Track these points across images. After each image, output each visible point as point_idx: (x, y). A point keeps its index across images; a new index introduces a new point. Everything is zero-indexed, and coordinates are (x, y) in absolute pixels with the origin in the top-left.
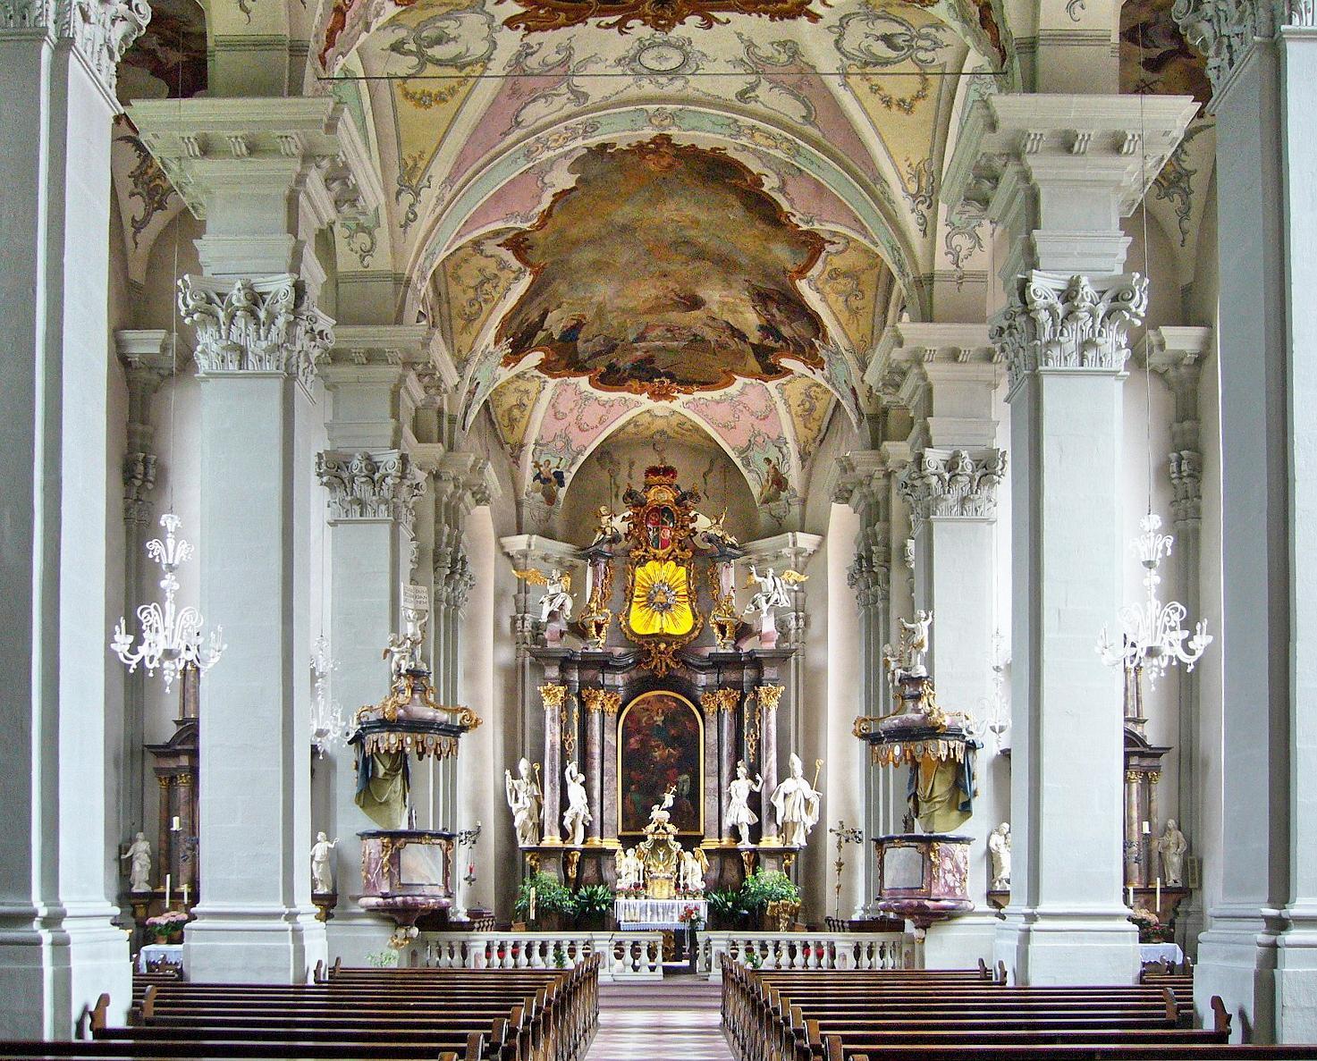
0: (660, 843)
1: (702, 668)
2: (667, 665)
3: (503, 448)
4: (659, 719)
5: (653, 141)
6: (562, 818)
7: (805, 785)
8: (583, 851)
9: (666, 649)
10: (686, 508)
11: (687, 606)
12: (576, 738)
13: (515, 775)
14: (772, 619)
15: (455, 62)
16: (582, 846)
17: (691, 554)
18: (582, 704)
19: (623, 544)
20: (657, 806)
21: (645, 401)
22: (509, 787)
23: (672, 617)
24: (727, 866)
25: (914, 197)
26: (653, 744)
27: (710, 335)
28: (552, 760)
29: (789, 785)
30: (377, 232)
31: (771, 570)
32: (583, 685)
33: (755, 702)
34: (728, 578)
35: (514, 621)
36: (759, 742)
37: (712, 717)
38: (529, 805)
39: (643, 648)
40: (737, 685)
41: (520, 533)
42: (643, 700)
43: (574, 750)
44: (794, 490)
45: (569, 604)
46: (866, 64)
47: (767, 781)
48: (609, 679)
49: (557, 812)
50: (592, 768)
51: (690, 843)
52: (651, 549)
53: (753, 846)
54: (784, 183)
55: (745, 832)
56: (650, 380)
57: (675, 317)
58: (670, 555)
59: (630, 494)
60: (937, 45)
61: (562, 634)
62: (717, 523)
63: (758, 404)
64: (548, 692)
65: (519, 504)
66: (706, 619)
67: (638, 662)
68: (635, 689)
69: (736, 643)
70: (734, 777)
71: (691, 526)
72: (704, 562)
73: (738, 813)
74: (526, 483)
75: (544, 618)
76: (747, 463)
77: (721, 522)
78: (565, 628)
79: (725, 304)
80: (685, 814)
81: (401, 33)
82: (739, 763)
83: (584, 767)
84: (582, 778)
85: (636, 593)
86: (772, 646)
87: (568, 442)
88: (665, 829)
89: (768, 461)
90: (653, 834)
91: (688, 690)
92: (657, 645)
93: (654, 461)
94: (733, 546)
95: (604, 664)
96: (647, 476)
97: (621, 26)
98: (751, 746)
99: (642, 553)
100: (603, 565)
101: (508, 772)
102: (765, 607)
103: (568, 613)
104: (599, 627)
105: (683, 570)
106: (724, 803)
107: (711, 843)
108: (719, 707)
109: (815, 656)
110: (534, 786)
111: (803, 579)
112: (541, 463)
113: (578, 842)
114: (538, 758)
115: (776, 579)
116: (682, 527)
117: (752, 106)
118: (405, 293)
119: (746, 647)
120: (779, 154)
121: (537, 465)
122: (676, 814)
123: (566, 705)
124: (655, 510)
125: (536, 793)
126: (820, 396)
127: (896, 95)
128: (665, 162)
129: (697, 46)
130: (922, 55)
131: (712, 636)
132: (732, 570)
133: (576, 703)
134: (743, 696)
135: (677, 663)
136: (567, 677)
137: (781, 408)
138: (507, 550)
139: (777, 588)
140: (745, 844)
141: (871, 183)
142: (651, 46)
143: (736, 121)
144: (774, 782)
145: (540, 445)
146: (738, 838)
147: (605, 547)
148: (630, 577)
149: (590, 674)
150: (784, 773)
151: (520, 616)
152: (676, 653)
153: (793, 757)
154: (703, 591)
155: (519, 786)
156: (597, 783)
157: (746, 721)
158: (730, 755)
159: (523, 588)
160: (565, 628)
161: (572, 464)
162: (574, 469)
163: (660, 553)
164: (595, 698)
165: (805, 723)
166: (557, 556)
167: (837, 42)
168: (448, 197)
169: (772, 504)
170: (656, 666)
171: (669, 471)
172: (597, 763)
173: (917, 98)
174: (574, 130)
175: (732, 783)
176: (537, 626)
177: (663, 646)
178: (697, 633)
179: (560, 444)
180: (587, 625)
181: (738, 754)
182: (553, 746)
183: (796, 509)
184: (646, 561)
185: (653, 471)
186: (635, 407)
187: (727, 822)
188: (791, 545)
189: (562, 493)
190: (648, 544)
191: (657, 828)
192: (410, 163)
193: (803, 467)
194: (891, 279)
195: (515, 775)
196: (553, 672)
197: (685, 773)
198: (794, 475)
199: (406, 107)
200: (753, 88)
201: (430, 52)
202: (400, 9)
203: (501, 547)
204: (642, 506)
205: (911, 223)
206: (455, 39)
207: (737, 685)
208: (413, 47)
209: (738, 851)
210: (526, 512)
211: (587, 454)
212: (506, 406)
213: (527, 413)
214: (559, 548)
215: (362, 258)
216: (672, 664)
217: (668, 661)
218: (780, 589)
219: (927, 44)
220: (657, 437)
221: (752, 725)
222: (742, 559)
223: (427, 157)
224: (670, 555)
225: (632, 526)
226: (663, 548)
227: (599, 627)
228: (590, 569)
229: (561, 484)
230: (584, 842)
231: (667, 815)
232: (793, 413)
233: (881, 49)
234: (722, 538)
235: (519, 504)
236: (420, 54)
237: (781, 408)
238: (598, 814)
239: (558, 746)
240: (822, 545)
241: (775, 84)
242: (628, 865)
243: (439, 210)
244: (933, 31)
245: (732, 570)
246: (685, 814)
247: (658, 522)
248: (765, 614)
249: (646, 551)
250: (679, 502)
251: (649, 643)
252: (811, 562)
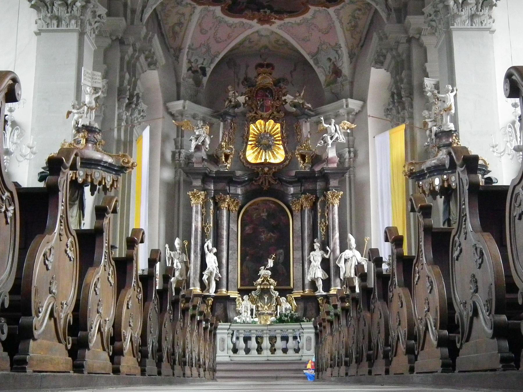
0: (265, 291)
1: (291, 183)
2: (269, 182)
3: (169, 51)
4: (264, 215)
6: (202, 275)
7: (358, 254)
8: (215, 298)
9: (268, 171)
10: (280, 88)
11: (281, 147)
12: (211, 225)
13: (172, 248)
14: (334, 150)
16: (214, 294)
17: (283, 115)
18: (216, 204)
19: (241, 109)
20: (263, 267)
21: (255, 25)
22: (168, 255)
23: (273, 153)
24: (309, 309)
26: (261, 230)
28: (196, 238)
29: (347, 253)
31: (333, 121)
32: (216, 191)
33: (326, 204)
34: (306, 128)
35: (174, 154)
36: (327, 227)
37: (297, 214)
38: (180, 267)
39: (255, 171)
40: (313, 192)
41: (178, 99)
42: (254, 203)
43: (211, 232)
44: (345, 76)
45: (208, 141)
47: (333, 251)
48: (232, 190)
49: (198, 272)
50: (222, 244)
51: (283, 293)
52: (260, 112)
53: (325, 293)
55: (320, 284)
56: (258, 10)
58: (270, 115)
59: (246, 79)
61: (203, 160)
62: (300, 95)
63: (321, 22)
64: (194, 196)
65: (178, 85)
66: (293, 154)
67: (250, 180)
68: (248, 196)
69: (312, 166)
70: (312, 249)
71: (283, 98)
72: (291, 121)
73: (316, 272)
74: (183, 75)
75: (192, 150)
76: (317, 62)
77: (302, 94)
78: (205, 157)
80: (281, 273)
82: (315, 240)
83: (217, 243)
84: (215, 250)
85: (250, 139)
86: (335, 165)
87: (208, 50)
88: (268, 281)
89: (330, 59)
90: (260, 284)
91: (282, 196)
92: (263, 169)
93: (259, 61)
94: (310, 109)
95: (229, 179)
96: (256, 68)
98: (323, 230)
99: (254, 115)
100: (229, 121)
101: (167, 246)
102: (330, 142)
103: (207, 146)
104: (227, 157)
105: (278, 125)
106: (306, 266)
107: (297, 293)
108: (302, 206)
109: (360, 174)
110: (184, 255)
111: (353, 126)
112: (192, 60)
113: (212, 291)
114: (187, 236)
115: (337, 126)
116: (278, 99)
119: (317, 169)
121: (190, 62)
122: (275, 272)
123: (205, 205)
124: (261, 88)
125: (185, 260)
126: (361, 17)
131: (297, 163)
132: (308, 124)
133: (212, 203)
134: (317, 199)
135: (275, 180)
136: (207, 187)
137: (337, 24)
138: (170, 111)
139: (336, 131)
140: (321, 292)
144: (338, 251)
145: (193, 49)
146: (315, 289)
147: (231, 111)
148: (246, 129)
149: (221, 186)
150: (344, 246)
151: (177, 151)
152: (274, 174)
153: (350, 236)
154: (290, 138)
155: (174, 255)
156: (225, 254)
157: (319, 214)
158: (309, 236)
159: (180, 133)
160: (205, 157)
161: (212, 62)
162: (213, 66)
163: (265, 114)
164: (224, 200)
165: (357, 216)
166: (201, 115)
169: (333, 86)
170: (262, 183)
171: (268, 65)
172: (225, 241)
175: (311, 253)
176: (189, 157)
177: (266, 169)
178: (287, 162)
179: (204, 50)
180: (219, 155)
181: (314, 234)
182: (196, 229)
183: (347, 87)
184: (257, 120)
185: (261, 65)
186: (248, 29)
187: (308, 278)
188: (345, 106)
189: (205, 80)
190: (257, 108)
191: (263, 281)
193: (351, 62)
195: (172, 248)
196: (198, 183)
197: (281, 248)
198: (346, 68)
203: (167, 109)
204: (253, 86)
207: (313, 192)
209: (316, 298)
210: (182, 89)
211: (221, 56)
212: (171, 24)
213: (183, 29)
214: (202, 110)
216: (272, 182)
217: (270, 180)
218: (339, 132)
220: (263, 51)
221: (323, 216)
222: (314, 119)
224: (270, 115)
225: (247, 98)
226: (266, 111)
227: (227, 157)
228: (222, 123)
229: (204, 74)
230: (215, 292)
231: (269, 273)
232: (345, 28)
234: (303, 104)
235: (178, 85)
237: (337, 24)
238: (225, 274)
239: (200, 229)
240: (364, 107)
242: (245, 305)
245: (308, 124)
246: (281, 273)
247: (264, 100)
248: (330, 146)
249: (256, 113)
250: (277, 83)
251: (258, 168)
252: (357, 117)
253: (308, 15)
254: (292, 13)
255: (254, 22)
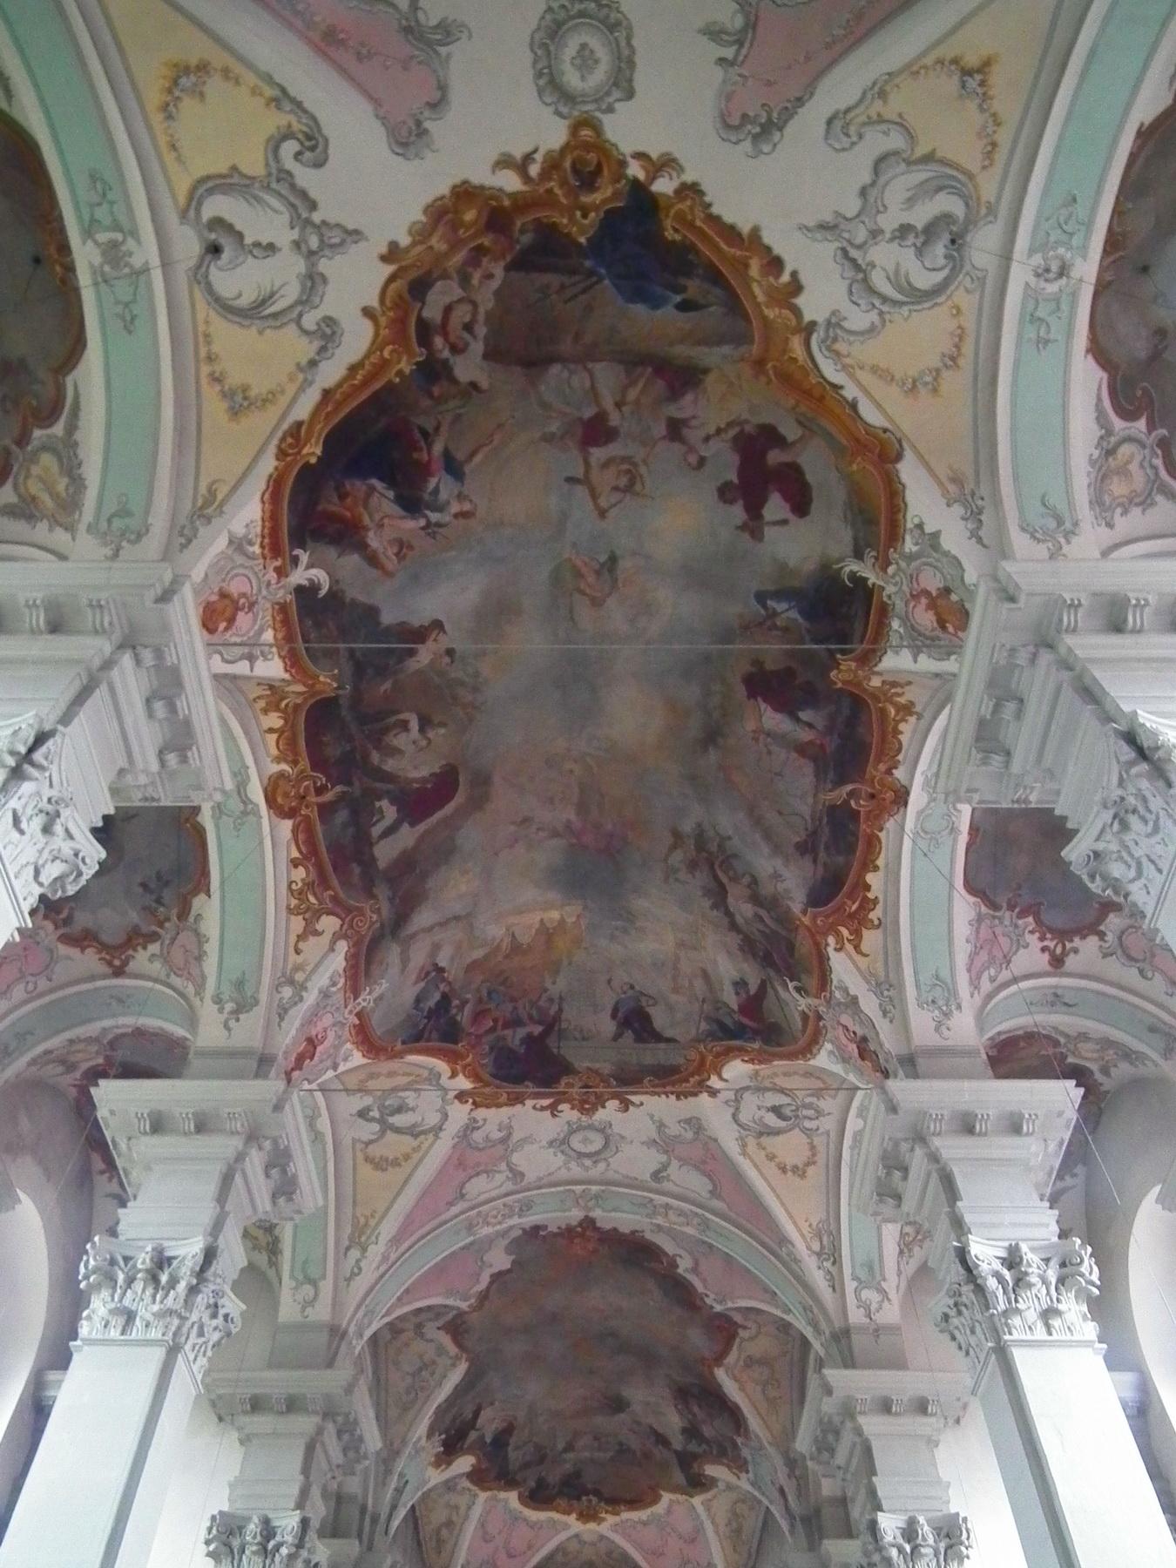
5: (580, 1224)
15: (413, 1131)
25: (819, 1255)
27: (634, 1443)
30: (321, 1284)
46: (761, 1134)
54: (696, 1263)
57: (600, 1421)
60: (819, 1113)
79: (648, 1404)
81: (368, 1100)
97: (553, 1109)
117: (667, 1186)
118: (338, 1347)
120: (689, 1230)
127: (790, 1161)
128: (590, 1246)
129: (616, 1129)
130: (807, 1124)
141: (776, 1243)
142: (580, 1128)
143: (652, 1200)
167: (734, 1116)
168: (393, 1257)
173: (808, 1164)
174: (511, 1208)
192: (362, 1220)
194: (805, 1343)
199: (366, 1171)
200: (665, 1167)
201: (391, 1120)
202: (365, 1061)
205: (818, 1279)
206: (413, 1109)
208: (375, 1114)
215: (303, 1309)
219: (810, 1113)
223: (377, 1216)
233: (772, 1120)
236: (382, 1121)
241: (684, 1161)
243: (382, 1269)
244: (814, 1100)
253: (659, 1509)
254: (635, 1503)
255: (572, 1519)
